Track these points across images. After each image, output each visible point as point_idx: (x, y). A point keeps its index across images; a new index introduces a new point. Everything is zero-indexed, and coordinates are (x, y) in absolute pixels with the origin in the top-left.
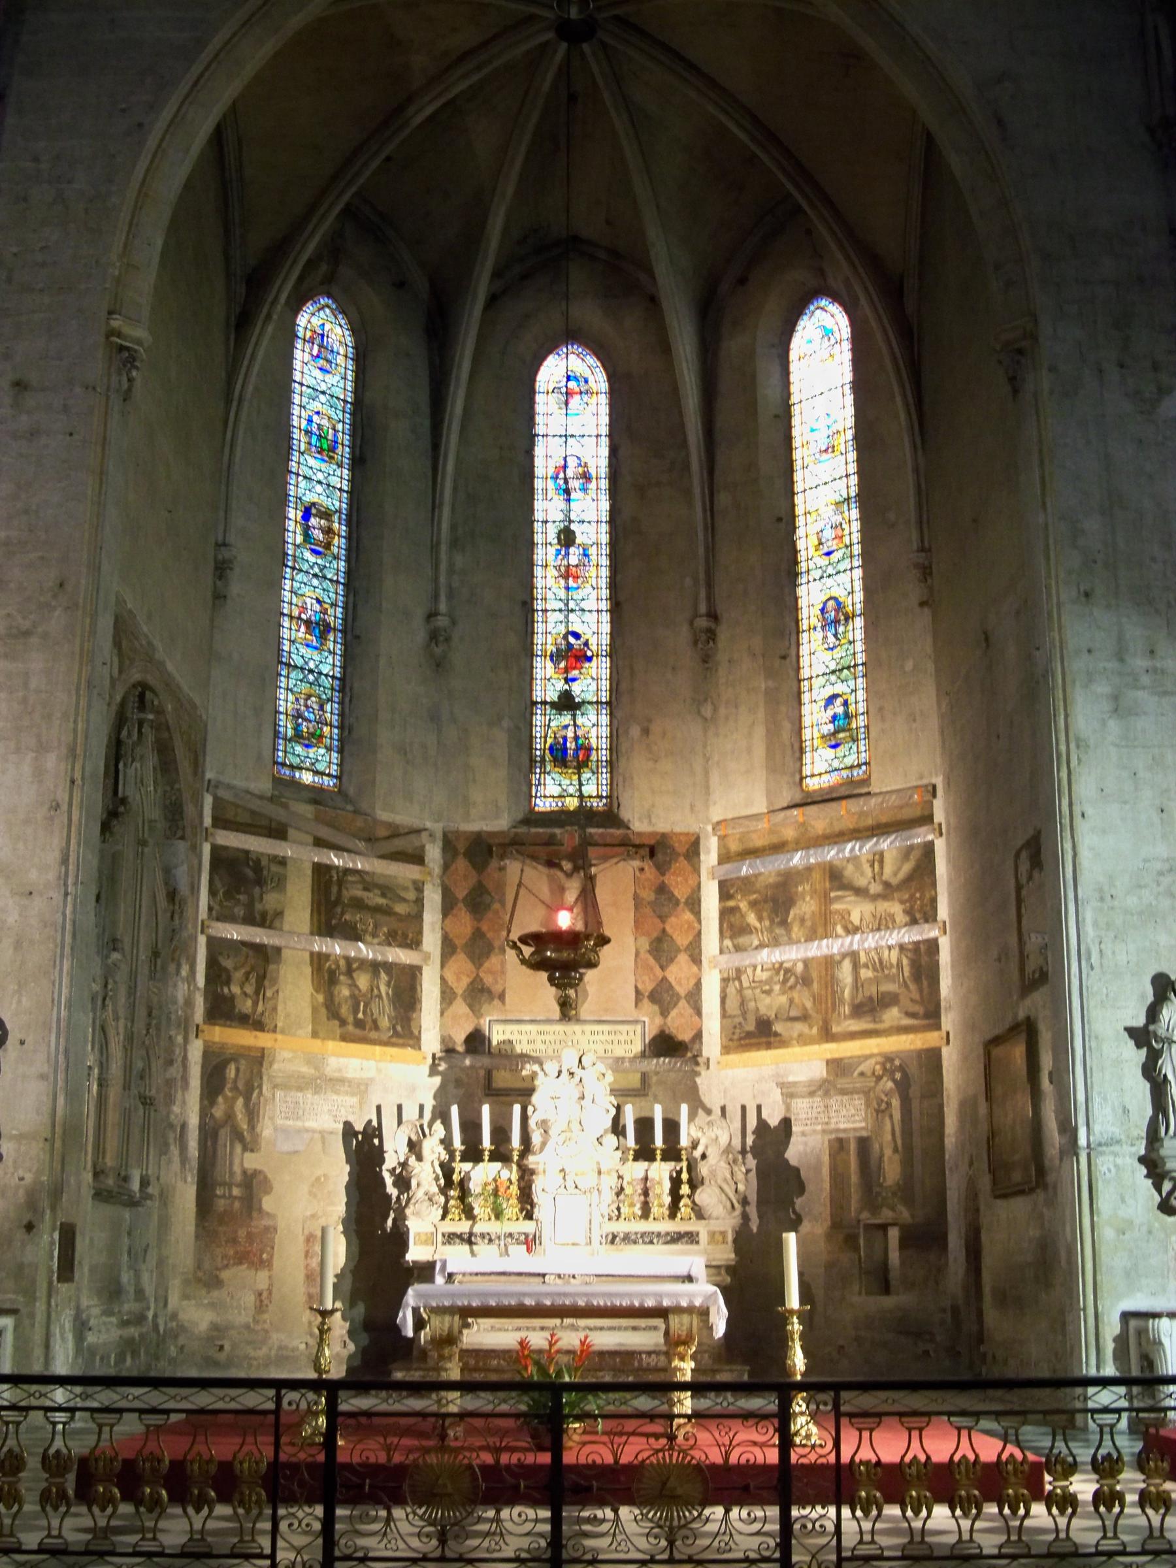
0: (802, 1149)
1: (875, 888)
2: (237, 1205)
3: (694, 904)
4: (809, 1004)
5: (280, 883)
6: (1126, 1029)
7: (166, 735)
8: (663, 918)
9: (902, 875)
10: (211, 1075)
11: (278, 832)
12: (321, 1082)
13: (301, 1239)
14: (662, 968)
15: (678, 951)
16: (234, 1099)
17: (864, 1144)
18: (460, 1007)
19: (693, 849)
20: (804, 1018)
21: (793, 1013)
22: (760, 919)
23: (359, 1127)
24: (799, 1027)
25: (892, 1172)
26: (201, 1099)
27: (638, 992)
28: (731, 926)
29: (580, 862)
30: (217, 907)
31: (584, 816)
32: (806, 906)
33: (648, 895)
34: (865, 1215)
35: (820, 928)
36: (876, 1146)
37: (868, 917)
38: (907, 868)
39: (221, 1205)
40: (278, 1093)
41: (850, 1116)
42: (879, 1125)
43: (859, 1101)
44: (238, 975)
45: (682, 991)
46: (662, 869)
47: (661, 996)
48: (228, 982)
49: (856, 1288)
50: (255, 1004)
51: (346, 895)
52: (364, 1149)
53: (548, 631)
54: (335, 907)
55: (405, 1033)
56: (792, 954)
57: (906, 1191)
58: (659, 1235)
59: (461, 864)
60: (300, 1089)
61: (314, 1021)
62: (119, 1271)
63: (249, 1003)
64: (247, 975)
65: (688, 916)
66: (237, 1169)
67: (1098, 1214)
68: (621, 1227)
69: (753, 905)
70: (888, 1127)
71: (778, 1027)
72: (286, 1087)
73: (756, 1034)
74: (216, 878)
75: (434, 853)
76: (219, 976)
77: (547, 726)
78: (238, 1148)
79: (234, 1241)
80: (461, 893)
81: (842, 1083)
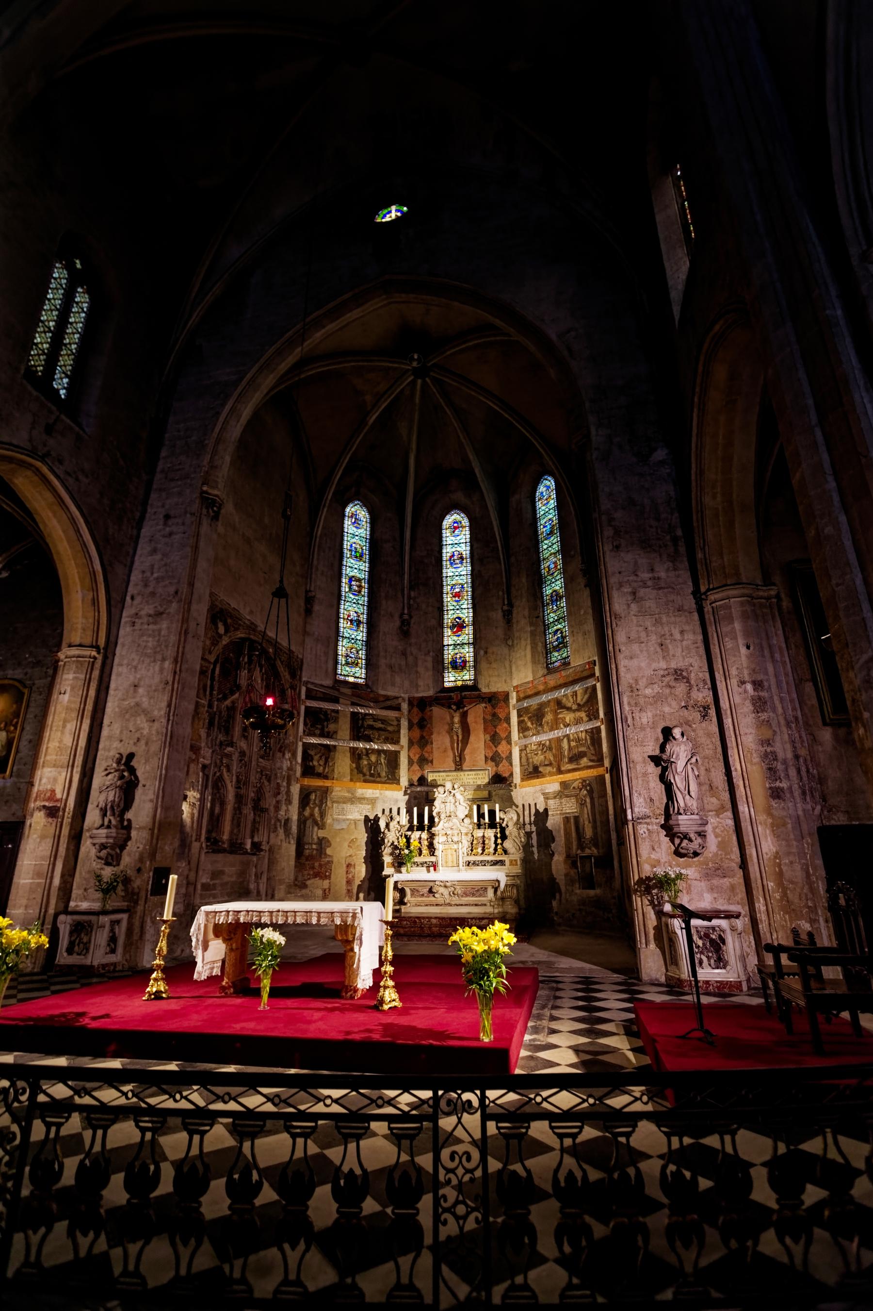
0: (553, 821)
1: (575, 707)
2: (315, 852)
3: (508, 720)
4: (552, 759)
5: (336, 720)
6: (649, 757)
8: (495, 727)
9: (584, 700)
11: (336, 700)
12: (353, 800)
13: (345, 866)
14: (496, 747)
15: (502, 739)
16: (314, 808)
17: (576, 819)
18: (416, 767)
19: (506, 696)
20: (550, 764)
21: (546, 763)
22: (532, 724)
23: (372, 817)
24: (549, 769)
25: (589, 833)
27: (486, 757)
28: (522, 728)
29: (460, 705)
31: (464, 688)
32: (549, 717)
33: (489, 717)
34: (579, 852)
35: (554, 726)
36: (581, 820)
37: (572, 720)
38: (586, 697)
39: (307, 852)
40: (335, 805)
41: (570, 807)
42: (582, 810)
43: (573, 800)
44: (316, 757)
45: (504, 756)
46: (494, 707)
47: (495, 759)
48: (312, 760)
49: (577, 886)
50: (324, 768)
51: (366, 724)
52: (372, 827)
53: (449, 617)
54: (360, 729)
55: (393, 778)
56: (544, 738)
57: (595, 841)
58: (488, 862)
59: (415, 710)
60: (344, 803)
61: (351, 774)
62: (248, 882)
63: (322, 768)
64: (321, 757)
65: (505, 725)
66: (315, 837)
67: (641, 857)
68: (472, 858)
69: (529, 718)
70: (586, 812)
71: (541, 769)
72: (338, 802)
73: (533, 772)
75: (405, 706)
77: (449, 654)
78: (316, 829)
79: (313, 868)
80: (415, 721)
81: (566, 792)
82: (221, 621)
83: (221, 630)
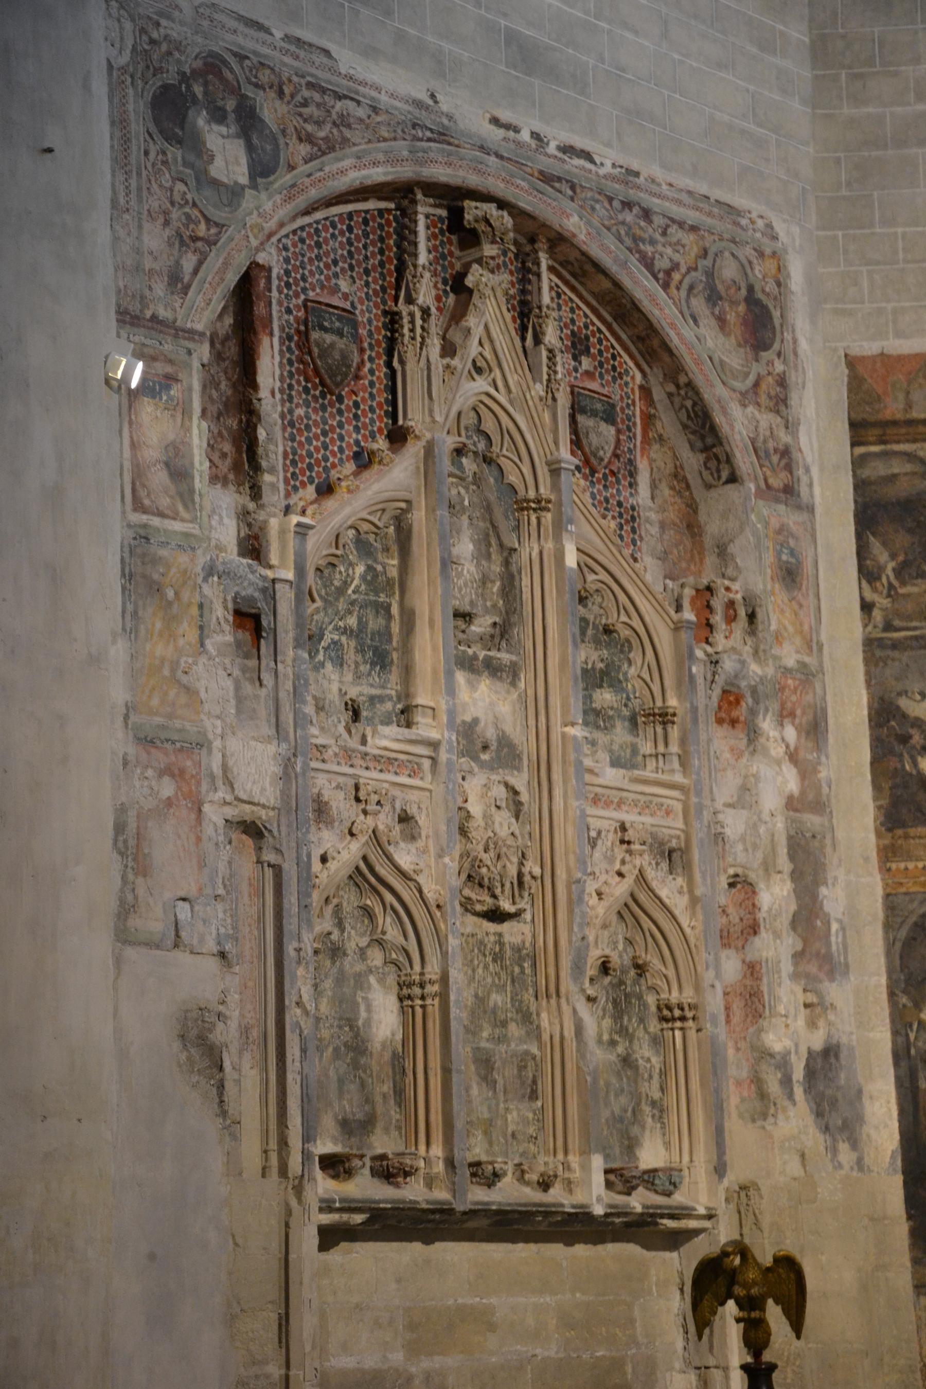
7: (607, 284)
10: (909, 943)
26: (891, 995)
30: (882, 601)
74: (875, 545)
76: (905, 739)
82: (218, 116)
83: (228, 157)
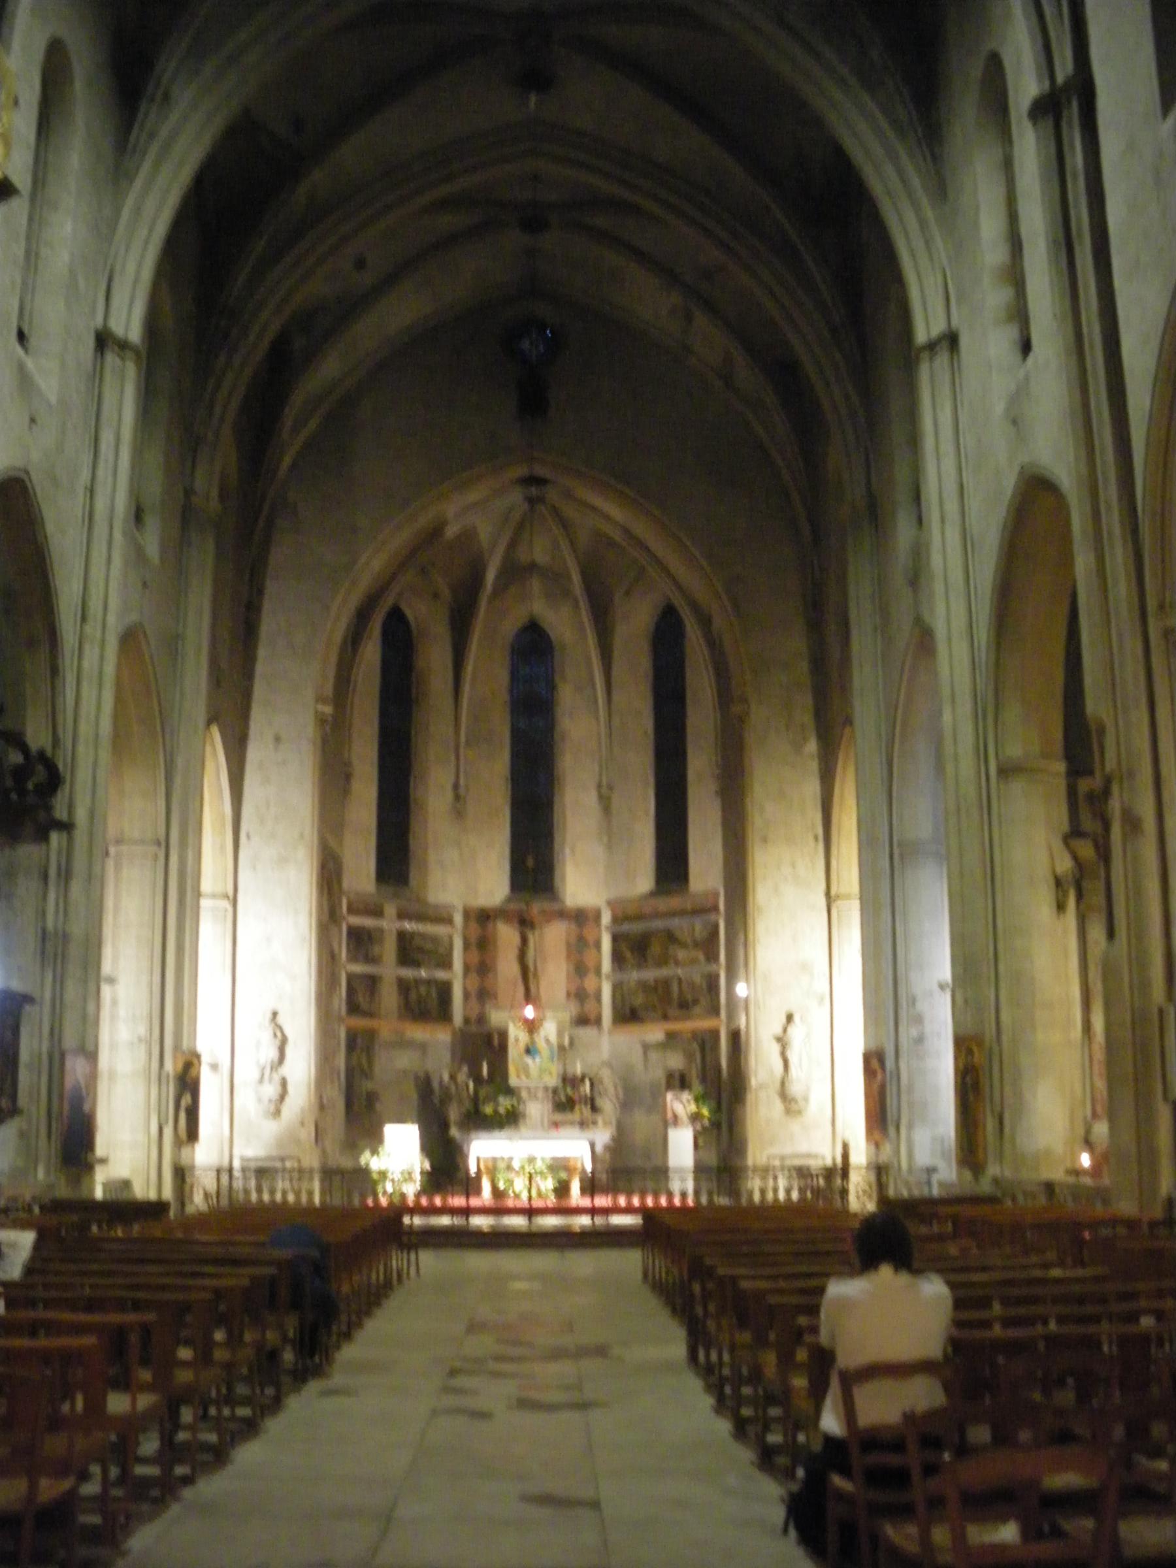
3: (598, 945)
5: (381, 941)
12: (403, 1043)
18: (474, 1001)
32: (655, 949)
35: (663, 961)
56: (650, 974)
75: (458, 919)
